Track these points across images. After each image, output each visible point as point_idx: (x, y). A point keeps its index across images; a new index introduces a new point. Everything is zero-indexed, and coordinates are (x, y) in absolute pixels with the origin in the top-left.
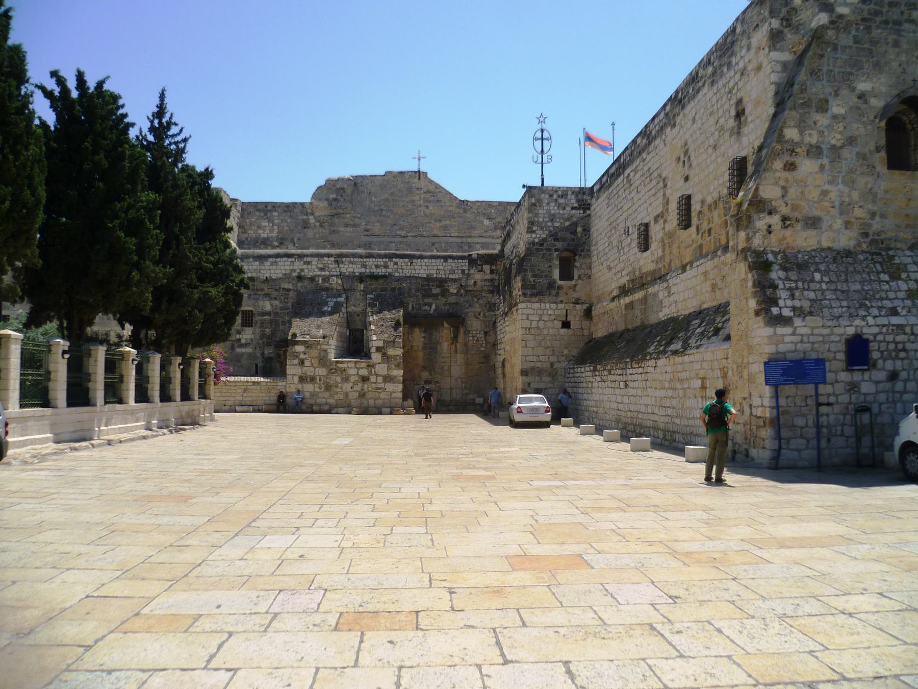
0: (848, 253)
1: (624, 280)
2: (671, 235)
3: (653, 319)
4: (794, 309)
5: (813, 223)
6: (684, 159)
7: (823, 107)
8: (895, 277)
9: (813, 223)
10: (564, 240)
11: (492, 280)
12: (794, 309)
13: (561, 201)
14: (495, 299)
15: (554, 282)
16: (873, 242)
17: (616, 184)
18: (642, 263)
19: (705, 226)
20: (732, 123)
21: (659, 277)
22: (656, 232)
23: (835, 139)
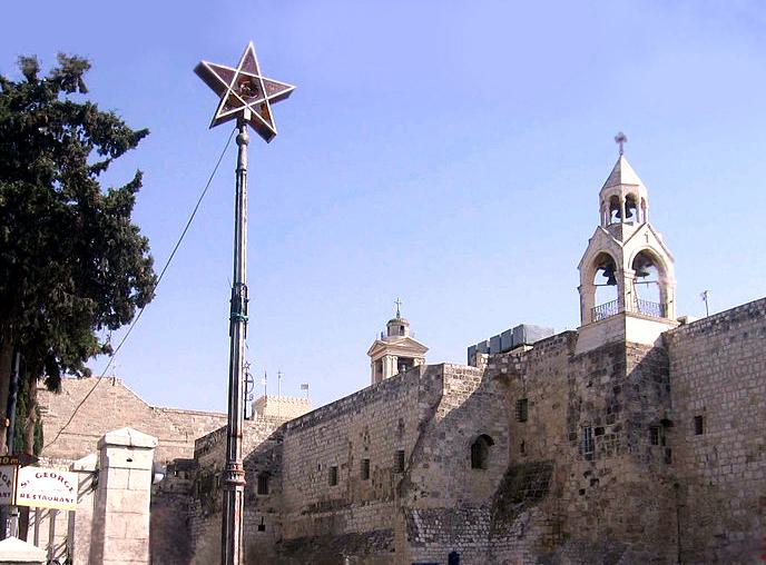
0: (451, 511)
1: (315, 501)
2: (354, 480)
3: (339, 532)
4: (426, 539)
5: (435, 495)
6: (365, 434)
7: (442, 436)
8: (473, 523)
9: (435, 495)
10: (262, 463)
11: (186, 484)
12: (426, 539)
13: (261, 432)
14: (190, 500)
15: (254, 495)
16: (464, 505)
17: (309, 431)
18: (330, 492)
19: (378, 482)
20: (396, 429)
21: (343, 504)
22: (342, 474)
23: (448, 453)
